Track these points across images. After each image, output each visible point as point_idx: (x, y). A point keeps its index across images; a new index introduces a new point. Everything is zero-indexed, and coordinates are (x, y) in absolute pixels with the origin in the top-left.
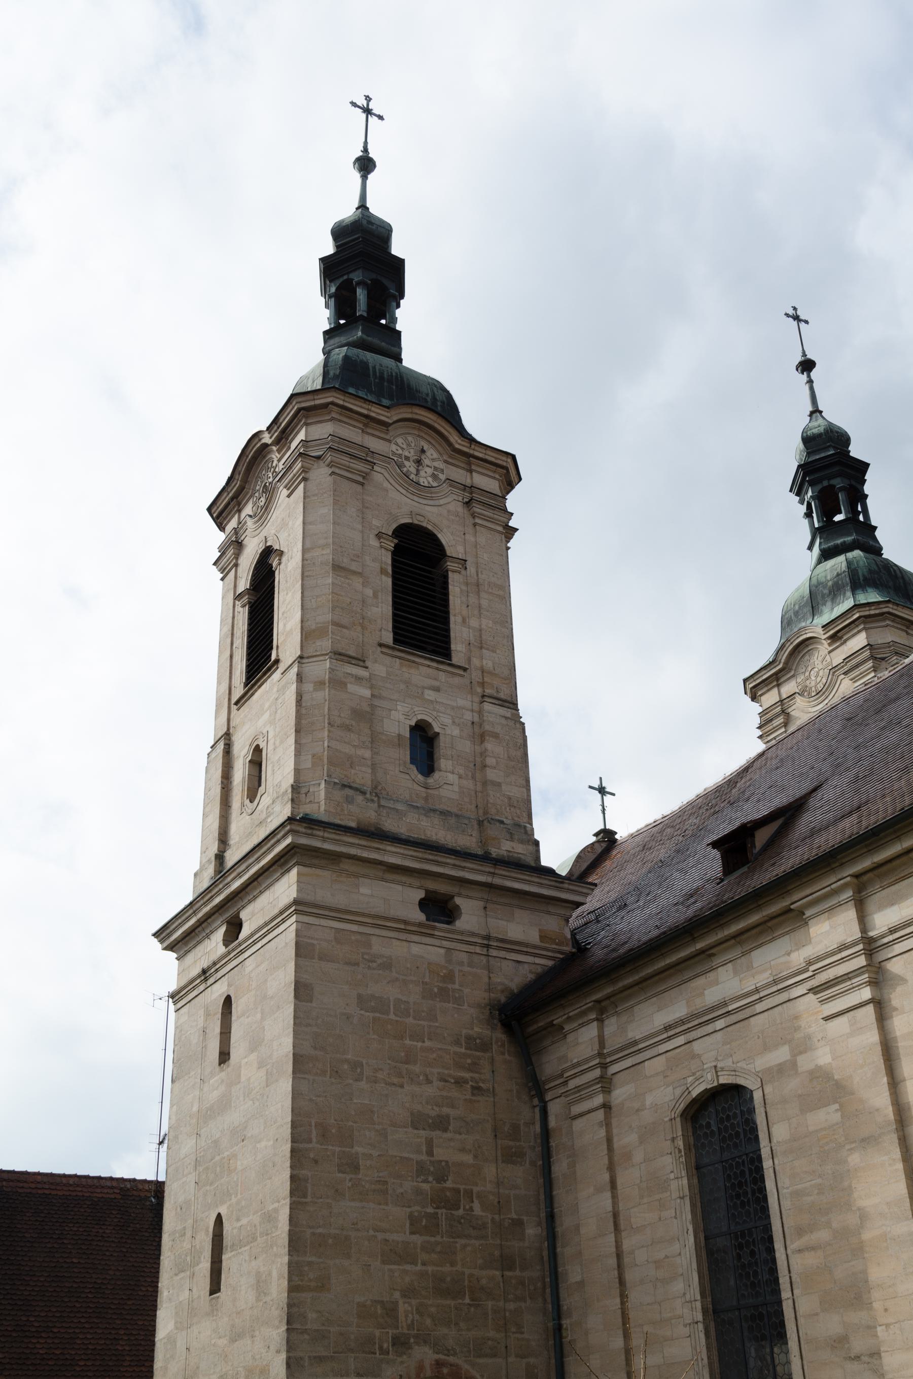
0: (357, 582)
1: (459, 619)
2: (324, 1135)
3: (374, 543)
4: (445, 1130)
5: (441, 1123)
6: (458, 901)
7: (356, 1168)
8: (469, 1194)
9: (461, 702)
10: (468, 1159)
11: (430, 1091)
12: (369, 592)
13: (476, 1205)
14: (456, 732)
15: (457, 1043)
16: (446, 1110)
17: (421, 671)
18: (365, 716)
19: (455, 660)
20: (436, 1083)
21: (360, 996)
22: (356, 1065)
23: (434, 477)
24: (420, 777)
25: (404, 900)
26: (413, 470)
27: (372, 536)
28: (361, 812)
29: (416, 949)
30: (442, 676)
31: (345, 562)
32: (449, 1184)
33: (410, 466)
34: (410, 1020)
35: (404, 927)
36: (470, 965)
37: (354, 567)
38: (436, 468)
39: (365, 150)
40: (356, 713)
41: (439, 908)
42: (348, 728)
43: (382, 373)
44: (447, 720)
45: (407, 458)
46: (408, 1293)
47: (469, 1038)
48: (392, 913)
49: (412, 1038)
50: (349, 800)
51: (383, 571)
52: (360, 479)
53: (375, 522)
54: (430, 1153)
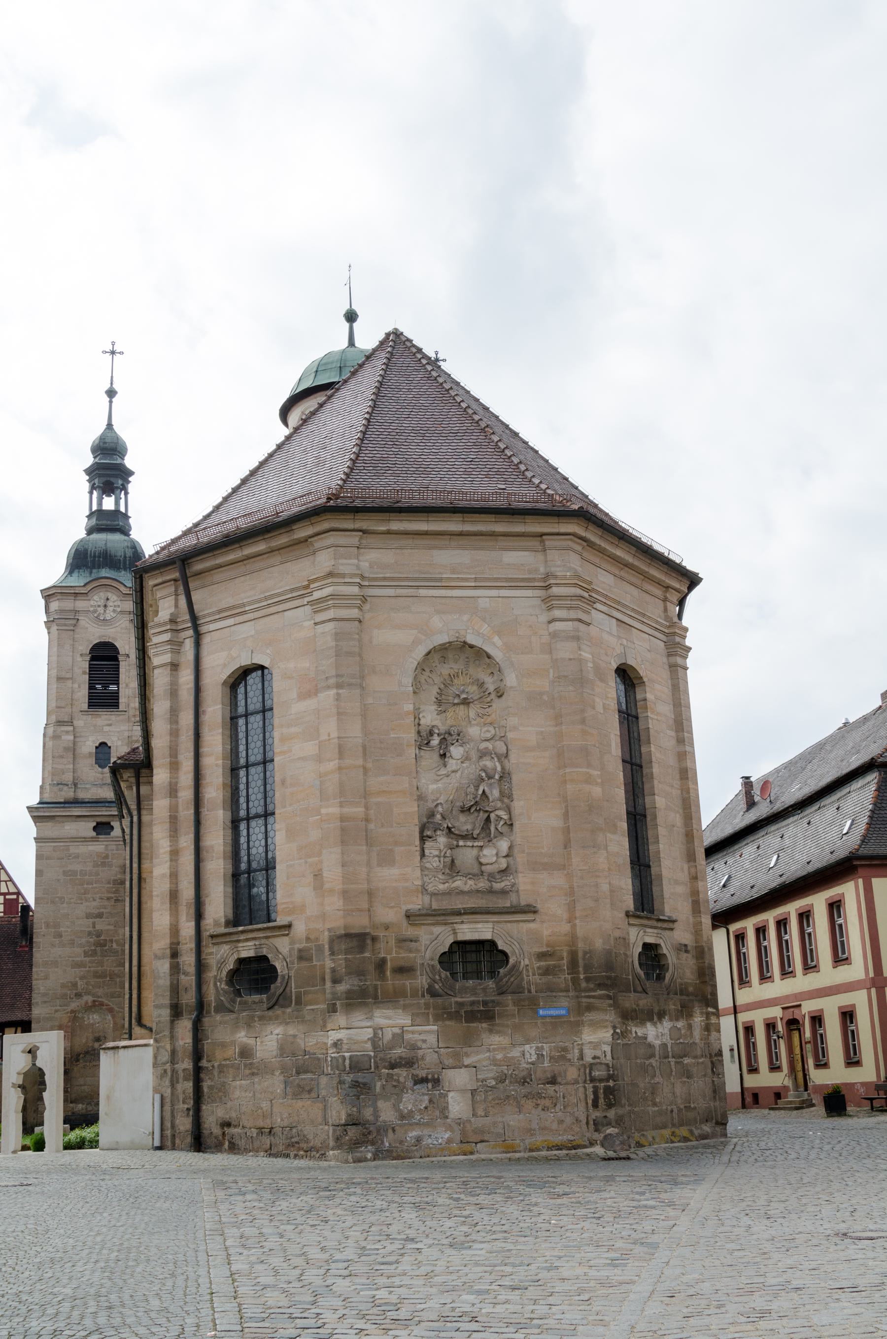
0: (69, 683)
1: (124, 685)
2: (48, 925)
3: (79, 659)
4: (101, 918)
5: (100, 916)
6: (112, 824)
7: (61, 936)
8: (111, 941)
9: (123, 728)
10: (112, 927)
11: (94, 904)
12: (76, 686)
13: (115, 946)
14: (120, 743)
15: (109, 883)
16: (102, 910)
17: (104, 718)
18: (73, 749)
19: (122, 707)
20: (98, 900)
21: (64, 871)
22: (61, 898)
23: (114, 611)
24: (100, 769)
25: (86, 828)
26: (102, 611)
27: (79, 656)
28: (68, 794)
29: (91, 848)
30: (113, 718)
31: (63, 674)
32: (102, 938)
33: (101, 610)
34: (87, 877)
35: (85, 840)
36: (117, 850)
37: (69, 675)
38: (115, 606)
39: (112, 384)
40: (66, 749)
41: (102, 828)
42: (62, 757)
43: (95, 553)
44: (115, 739)
45: (99, 606)
46: (82, 978)
47: (115, 881)
48: (80, 835)
49: (87, 884)
50: (60, 790)
51: (84, 673)
52: (72, 628)
53: (80, 648)
54: (94, 927)
